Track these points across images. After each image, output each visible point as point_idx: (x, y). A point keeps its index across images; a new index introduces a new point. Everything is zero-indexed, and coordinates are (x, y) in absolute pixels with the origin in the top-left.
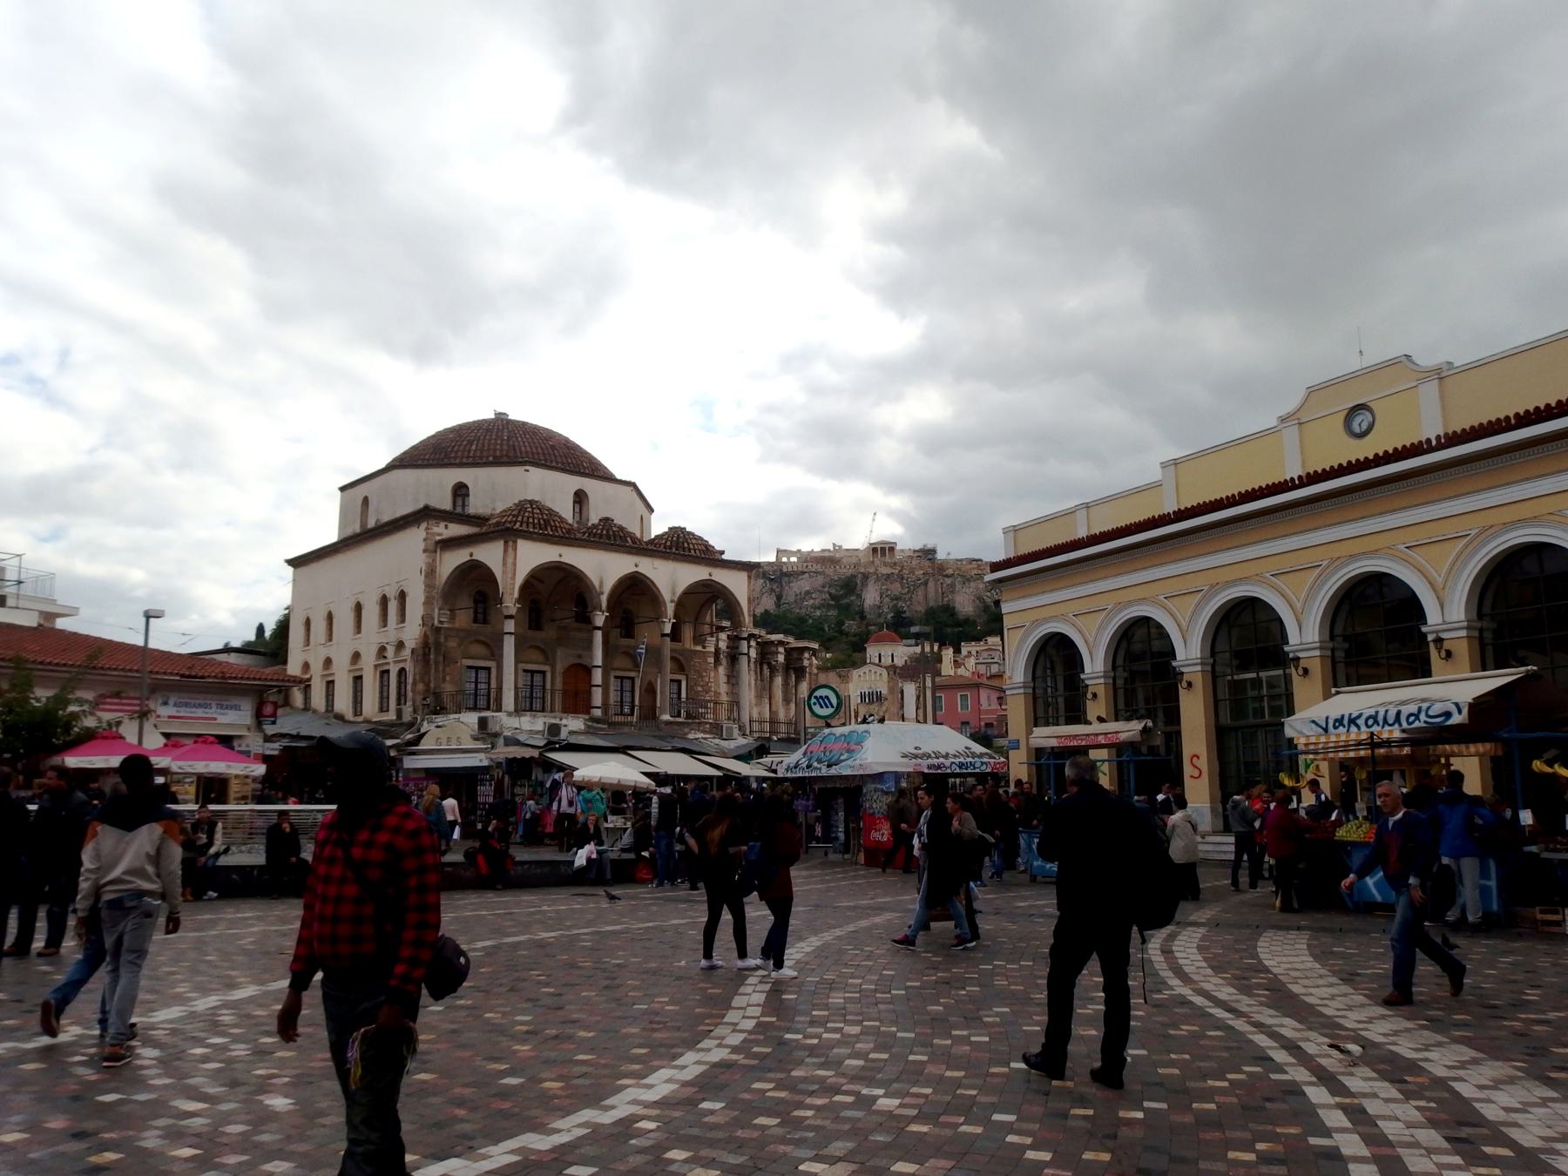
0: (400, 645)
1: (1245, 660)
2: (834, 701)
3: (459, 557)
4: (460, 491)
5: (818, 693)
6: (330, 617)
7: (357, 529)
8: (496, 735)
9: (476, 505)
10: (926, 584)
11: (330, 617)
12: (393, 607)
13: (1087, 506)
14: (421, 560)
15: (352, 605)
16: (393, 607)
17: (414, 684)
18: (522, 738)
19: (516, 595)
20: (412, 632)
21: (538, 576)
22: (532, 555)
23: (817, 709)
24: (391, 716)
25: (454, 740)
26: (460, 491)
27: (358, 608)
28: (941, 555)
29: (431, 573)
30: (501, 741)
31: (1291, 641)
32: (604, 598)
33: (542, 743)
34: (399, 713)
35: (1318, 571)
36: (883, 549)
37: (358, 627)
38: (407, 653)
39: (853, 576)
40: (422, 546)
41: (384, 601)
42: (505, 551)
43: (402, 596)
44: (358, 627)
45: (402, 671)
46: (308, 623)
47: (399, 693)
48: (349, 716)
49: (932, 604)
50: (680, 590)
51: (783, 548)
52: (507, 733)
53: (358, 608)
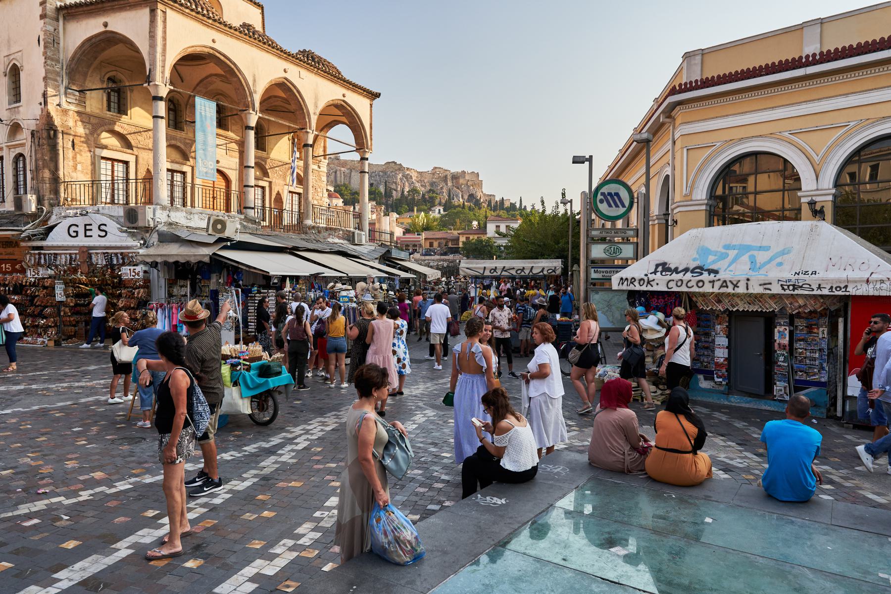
0: (16, 128)
2: (627, 204)
5: (605, 190)
8: (148, 229)
10: (336, 172)
13: (821, 22)
14: (38, 27)
17: (37, 170)
18: (183, 234)
19: (167, 74)
21: (191, 59)
23: (603, 207)
25: (95, 232)
29: (51, 43)
30: (154, 238)
31: (804, 187)
32: (257, 98)
33: (212, 240)
34: (19, 203)
35: (709, 151)
38: (24, 136)
40: (39, 11)
42: (153, 21)
47: (16, 182)
50: (321, 105)
52: (162, 228)
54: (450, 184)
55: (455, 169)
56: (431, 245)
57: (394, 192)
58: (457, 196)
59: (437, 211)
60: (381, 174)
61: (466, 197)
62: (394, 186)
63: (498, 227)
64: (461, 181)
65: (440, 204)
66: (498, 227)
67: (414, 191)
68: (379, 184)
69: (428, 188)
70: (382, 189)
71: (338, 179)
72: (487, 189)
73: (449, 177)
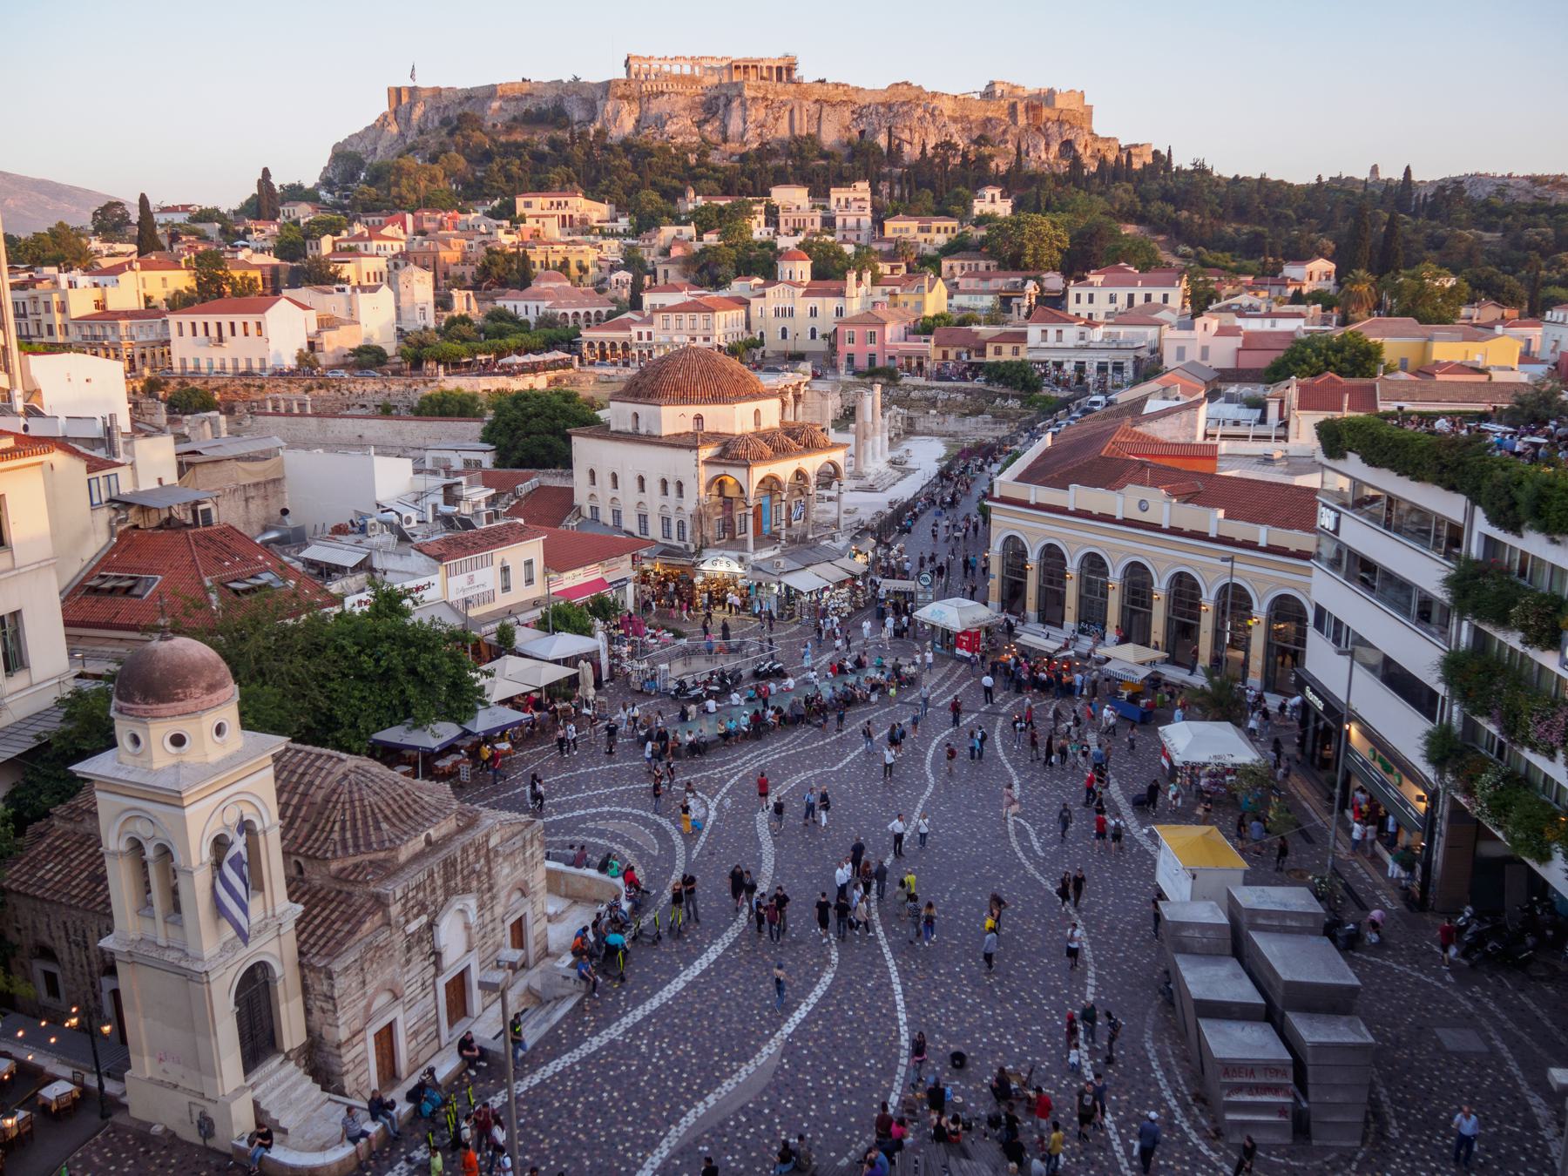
1: (1091, 572)
3: (719, 471)
4: (699, 418)
6: (615, 477)
7: (630, 428)
9: (708, 427)
11: (615, 477)
12: (672, 489)
15: (636, 474)
16: (672, 489)
17: (693, 533)
20: (689, 505)
22: (759, 472)
24: (675, 542)
26: (699, 418)
27: (641, 480)
28: (807, 73)
36: (746, 67)
37: (642, 489)
39: (717, 98)
41: (664, 483)
43: (680, 485)
44: (642, 489)
45: (681, 524)
46: (592, 473)
48: (637, 533)
49: (797, 132)
51: (634, 54)
53: (641, 480)
54: (1022, 120)
55: (1032, 83)
56: (945, 355)
57: (907, 148)
58: (1036, 147)
59: (989, 198)
60: (882, 110)
61: (1055, 148)
62: (906, 135)
63: (1045, 332)
64: (1046, 112)
65: (995, 185)
66: (1045, 332)
67: (948, 145)
68: (876, 132)
69: (976, 134)
70: (882, 140)
71: (797, 123)
72: (1101, 127)
73: (1021, 107)
